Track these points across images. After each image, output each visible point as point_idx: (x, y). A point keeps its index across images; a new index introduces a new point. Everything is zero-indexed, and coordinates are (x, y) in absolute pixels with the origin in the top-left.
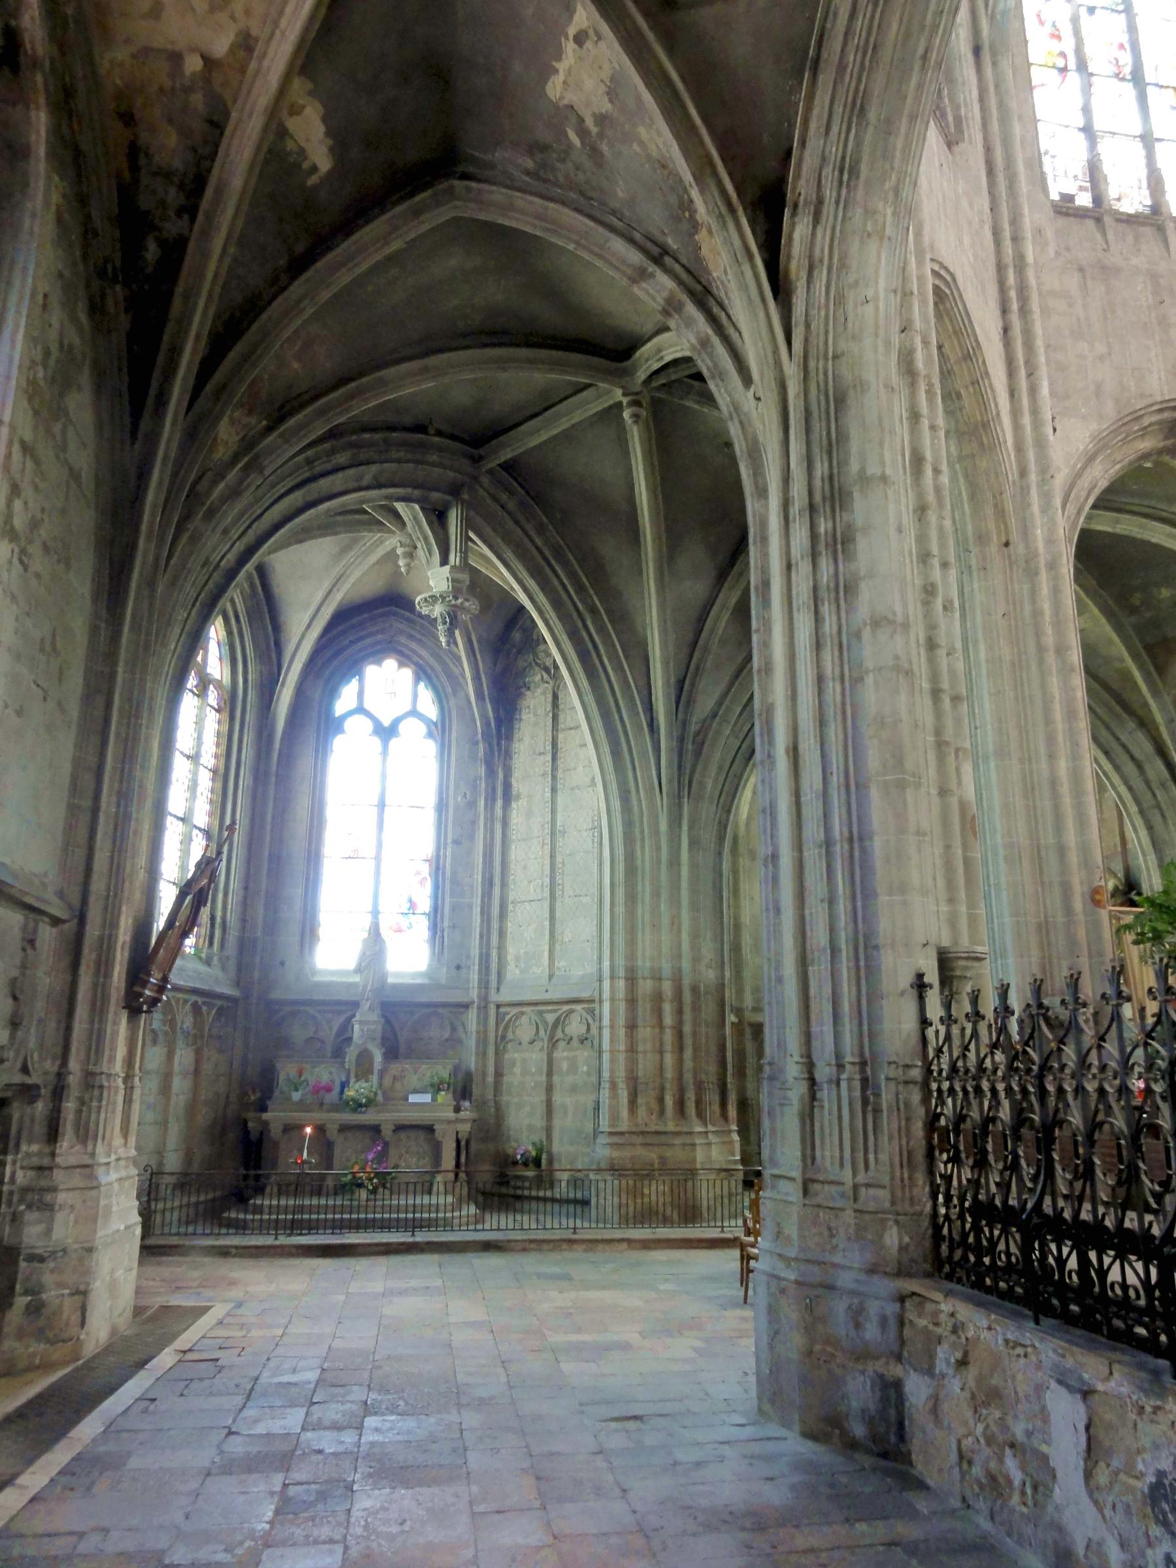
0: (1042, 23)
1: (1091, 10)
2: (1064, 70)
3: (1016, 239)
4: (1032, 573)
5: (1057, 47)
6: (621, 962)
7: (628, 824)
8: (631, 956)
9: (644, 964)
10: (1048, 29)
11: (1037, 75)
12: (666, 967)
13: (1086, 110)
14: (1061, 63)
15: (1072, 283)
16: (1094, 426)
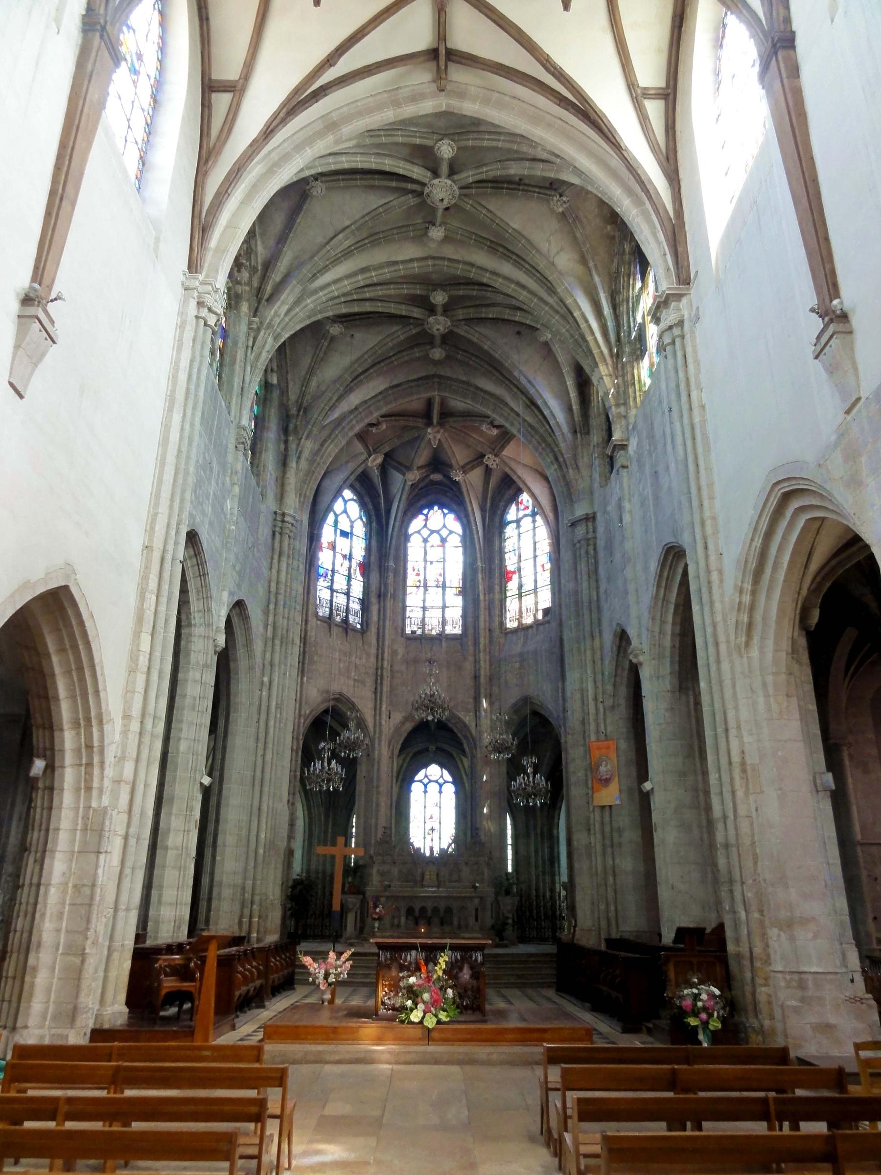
0: (414, 570)
1: (431, 563)
2: (417, 587)
3: (383, 659)
4: (373, 765)
5: (418, 578)
6: (305, 867)
7: (310, 818)
8: (309, 865)
9: (313, 867)
10: (416, 572)
11: (409, 590)
12: (321, 868)
13: (424, 601)
14: (418, 584)
15: (403, 668)
16: (404, 714)
